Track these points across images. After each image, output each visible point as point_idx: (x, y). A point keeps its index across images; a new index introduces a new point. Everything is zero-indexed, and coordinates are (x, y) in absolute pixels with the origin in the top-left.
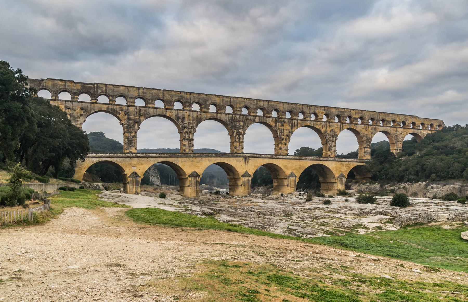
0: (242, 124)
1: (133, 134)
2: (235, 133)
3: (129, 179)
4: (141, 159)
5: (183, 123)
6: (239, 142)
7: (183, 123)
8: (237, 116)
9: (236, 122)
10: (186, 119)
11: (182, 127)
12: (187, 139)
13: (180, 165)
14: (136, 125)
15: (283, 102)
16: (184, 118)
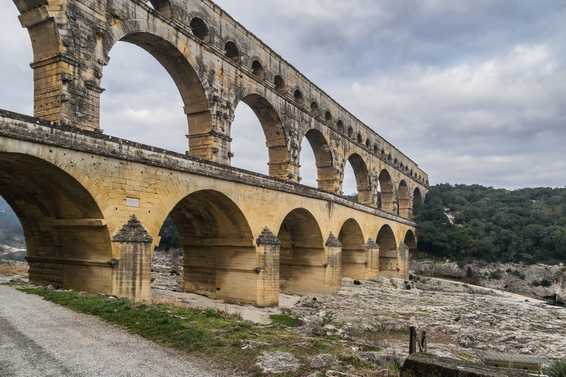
0: (297, 126)
1: (88, 75)
2: (289, 143)
3: (118, 250)
4: (152, 170)
5: (211, 85)
6: (295, 165)
7: (211, 85)
8: (291, 105)
9: (290, 118)
10: (216, 77)
11: (210, 95)
12: (220, 136)
13: (242, 206)
14: (99, 44)
15: (334, 101)
16: (213, 72)
